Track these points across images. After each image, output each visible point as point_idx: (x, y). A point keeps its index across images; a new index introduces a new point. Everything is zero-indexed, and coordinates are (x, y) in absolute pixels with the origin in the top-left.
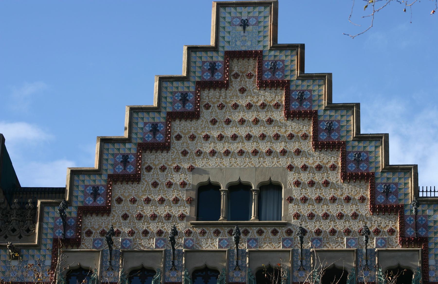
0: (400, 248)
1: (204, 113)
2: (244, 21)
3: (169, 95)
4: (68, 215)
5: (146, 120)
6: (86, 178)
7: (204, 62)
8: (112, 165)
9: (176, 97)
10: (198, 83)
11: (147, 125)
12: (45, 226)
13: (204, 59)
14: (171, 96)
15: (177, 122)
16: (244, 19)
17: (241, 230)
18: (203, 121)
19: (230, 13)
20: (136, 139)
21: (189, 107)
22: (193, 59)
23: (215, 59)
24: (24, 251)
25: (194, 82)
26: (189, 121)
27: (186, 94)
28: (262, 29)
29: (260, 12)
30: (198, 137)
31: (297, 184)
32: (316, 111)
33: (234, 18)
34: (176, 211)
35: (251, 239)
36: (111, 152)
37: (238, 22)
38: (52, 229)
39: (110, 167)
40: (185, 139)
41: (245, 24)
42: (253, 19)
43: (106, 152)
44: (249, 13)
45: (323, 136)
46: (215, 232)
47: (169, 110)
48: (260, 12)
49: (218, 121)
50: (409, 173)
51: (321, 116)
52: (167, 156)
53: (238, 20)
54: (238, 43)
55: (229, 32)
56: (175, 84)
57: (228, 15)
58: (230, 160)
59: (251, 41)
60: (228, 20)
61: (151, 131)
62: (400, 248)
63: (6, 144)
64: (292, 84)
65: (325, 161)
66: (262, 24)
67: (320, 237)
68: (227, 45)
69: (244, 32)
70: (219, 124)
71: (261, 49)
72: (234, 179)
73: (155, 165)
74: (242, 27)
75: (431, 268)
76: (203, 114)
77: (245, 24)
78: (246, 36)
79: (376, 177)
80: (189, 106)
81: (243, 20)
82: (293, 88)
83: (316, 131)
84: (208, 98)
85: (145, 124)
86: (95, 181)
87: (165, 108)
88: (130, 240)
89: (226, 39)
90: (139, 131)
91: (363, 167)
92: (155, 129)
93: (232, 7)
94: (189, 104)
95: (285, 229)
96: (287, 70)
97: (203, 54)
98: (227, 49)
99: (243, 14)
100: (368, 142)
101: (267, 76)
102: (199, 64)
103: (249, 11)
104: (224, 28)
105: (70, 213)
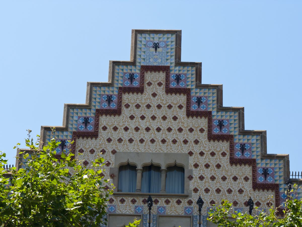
1: (124, 110)
2: (156, 44)
3: (98, 96)
5: (79, 115)
7: (125, 73)
9: (103, 98)
11: (81, 119)
13: (125, 71)
14: (99, 97)
15: (104, 116)
16: (156, 42)
17: (153, 199)
18: (123, 117)
19: (145, 38)
20: (72, 128)
21: (114, 106)
22: (116, 71)
23: (133, 71)
25: (117, 88)
26: (113, 116)
27: (111, 96)
28: (169, 50)
29: (168, 38)
30: (120, 129)
31: (196, 166)
32: (210, 113)
33: (148, 42)
35: (160, 207)
37: (152, 45)
40: (110, 129)
41: (156, 46)
42: (162, 43)
44: (160, 38)
45: (216, 130)
47: (97, 108)
48: (168, 38)
49: (135, 117)
50: (282, 160)
51: (214, 116)
52: (96, 142)
53: (151, 43)
54: (151, 60)
55: (144, 52)
56: (103, 89)
57: (143, 39)
58: (144, 146)
59: (161, 59)
60: (143, 43)
61: (83, 123)
64: (192, 91)
65: (218, 150)
66: (169, 47)
68: (142, 61)
69: (156, 52)
70: (136, 119)
71: (169, 65)
72: (148, 161)
73: (85, 148)
74: (155, 48)
76: (124, 111)
77: (156, 46)
78: (157, 55)
79: (257, 162)
80: (113, 105)
81: (155, 43)
82: (193, 94)
84: (128, 100)
87: (95, 106)
89: (142, 57)
90: (75, 122)
92: (86, 121)
93: (147, 33)
94: (113, 104)
95: (186, 200)
96: (188, 81)
97: (125, 67)
98: (142, 64)
99: (155, 39)
100: (251, 136)
101: (173, 85)
102: (121, 75)
103: (160, 37)
104: (141, 48)
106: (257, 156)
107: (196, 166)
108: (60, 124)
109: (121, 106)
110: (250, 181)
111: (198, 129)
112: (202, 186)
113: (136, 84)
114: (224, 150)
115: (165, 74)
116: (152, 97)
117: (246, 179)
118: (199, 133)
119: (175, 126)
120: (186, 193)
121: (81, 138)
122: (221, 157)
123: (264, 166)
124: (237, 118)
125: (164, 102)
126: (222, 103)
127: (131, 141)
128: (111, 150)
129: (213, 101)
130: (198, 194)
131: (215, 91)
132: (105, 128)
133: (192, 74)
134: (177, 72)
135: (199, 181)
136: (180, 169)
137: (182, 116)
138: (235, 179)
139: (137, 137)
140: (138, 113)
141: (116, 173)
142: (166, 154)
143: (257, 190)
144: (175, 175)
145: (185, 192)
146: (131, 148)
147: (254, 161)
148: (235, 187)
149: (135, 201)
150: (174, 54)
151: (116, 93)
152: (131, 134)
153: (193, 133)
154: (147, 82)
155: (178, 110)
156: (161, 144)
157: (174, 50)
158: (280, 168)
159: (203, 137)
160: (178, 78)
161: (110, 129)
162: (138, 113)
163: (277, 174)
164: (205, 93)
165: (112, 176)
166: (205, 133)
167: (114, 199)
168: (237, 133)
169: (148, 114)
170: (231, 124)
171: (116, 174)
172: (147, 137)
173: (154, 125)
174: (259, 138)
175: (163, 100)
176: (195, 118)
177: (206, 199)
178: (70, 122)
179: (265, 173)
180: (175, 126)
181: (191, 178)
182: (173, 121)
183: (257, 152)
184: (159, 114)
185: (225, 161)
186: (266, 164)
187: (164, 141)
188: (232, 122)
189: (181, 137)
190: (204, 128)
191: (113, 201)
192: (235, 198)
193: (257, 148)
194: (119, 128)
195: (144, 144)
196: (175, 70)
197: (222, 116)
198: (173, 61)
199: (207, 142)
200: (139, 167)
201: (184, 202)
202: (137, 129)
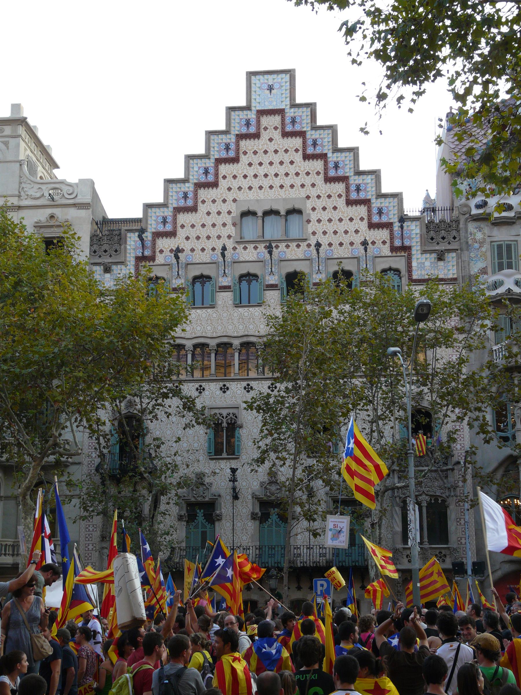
0: (390, 254)
3: (216, 145)
4: (145, 239)
5: (199, 165)
6: (157, 210)
7: (241, 119)
8: (176, 200)
10: (237, 135)
12: (128, 247)
13: (241, 117)
15: (223, 165)
17: (274, 245)
19: (259, 80)
21: (232, 154)
22: (233, 117)
23: (249, 117)
24: (114, 267)
28: (284, 92)
31: (314, 209)
33: (262, 84)
34: (225, 232)
36: (174, 190)
38: (134, 249)
39: (175, 202)
40: (229, 178)
41: (271, 88)
43: (170, 190)
45: (332, 172)
46: (254, 248)
47: (217, 157)
48: (282, 79)
54: (266, 103)
57: (258, 82)
60: (257, 85)
62: (390, 254)
63: (96, 186)
65: (334, 191)
66: (284, 88)
67: (332, 248)
68: (258, 105)
72: (267, 208)
73: (207, 199)
75: (414, 268)
77: (271, 88)
82: (308, 136)
83: (326, 169)
85: (199, 168)
86: (164, 212)
87: (214, 155)
88: (192, 256)
89: (257, 100)
90: (195, 173)
91: (363, 195)
92: (206, 172)
95: (305, 243)
97: (240, 112)
98: (258, 108)
102: (237, 121)
104: (255, 92)
105: (147, 237)
106: (372, 195)
107: (314, 209)
108: (181, 175)
109: (238, 153)
110: (366, 221)
111: (315, 172)
112: (319, 228)
113: (252, 130)
114: (340, 192)
115: (280, 117)
116: (268, 143)
117: (362, 219)
118: (316, 176)
119: (292, 170)
120: (305, 238)
121: (202, 189)
122: (338, 199)
123: (379, 205)
124: (352, 158)
125: (281, 147)
126: (337, 144)
127: (250, 188)
128: (232, 199)
129: (328, 142)
130: (316, 236)
131: (330, 131)
132: (224, 177)
133: (307, 116)
134: (292, 115)
135: (317, 224)
136: (299, 212)
137: (298, 160)
138: (351, 220)
139: (255, 184)
140: (256, 160)
141: (238, 221)
142: (284, 200)
143: (372, 230)
144: (294, 219)
145: (304, 235)
146: (251, 195)
147: (369, 201)
148: (351, 227)
149: (257, 248)
150: (288, 95)
151: (233, 140)
152: (250, 181)
153: (310, 176)
154: (263, 127)
155: (294, 153)
156: (280, 190)
157: (288, 91)
158: (394, 206)
159: (320, 180)
160: (293, 121)
161: (229, 178)
162: (256, 160)
163: (392, 212)
164: (320, 135)
165: (234, 224)
166: (322, 176)
167: (237, 246)
168: (352, 174)
169: (266, 159)
170: (346, 165)
171: (238, 222)
172: (266, 183)
173: (272, 171)
174: (373, 177)
175: (279, 145)
176: (311, 160)
177: (324, 241)
178: (191, 173)
179: (380, 212)
180: (292, 170)
181: (309, 221)
182: (290, 165)
183: (372, 191)
184: (276, 159)
185: (341, 203)
186: (381, 203)
187: (282, 187)
188: (348, 162)
189: (298, 181)
190: (320, 171)
191: (236, 248)
192: (352, 239)
193: (372, 187)
194: (238, 176)
195: (263, 190)
196: (290, 113)
197: (337, 157)
198: (288, 103)
199: (324, 185)
200: (260, 214)
201: (303, 245)
202: (255, 176)
